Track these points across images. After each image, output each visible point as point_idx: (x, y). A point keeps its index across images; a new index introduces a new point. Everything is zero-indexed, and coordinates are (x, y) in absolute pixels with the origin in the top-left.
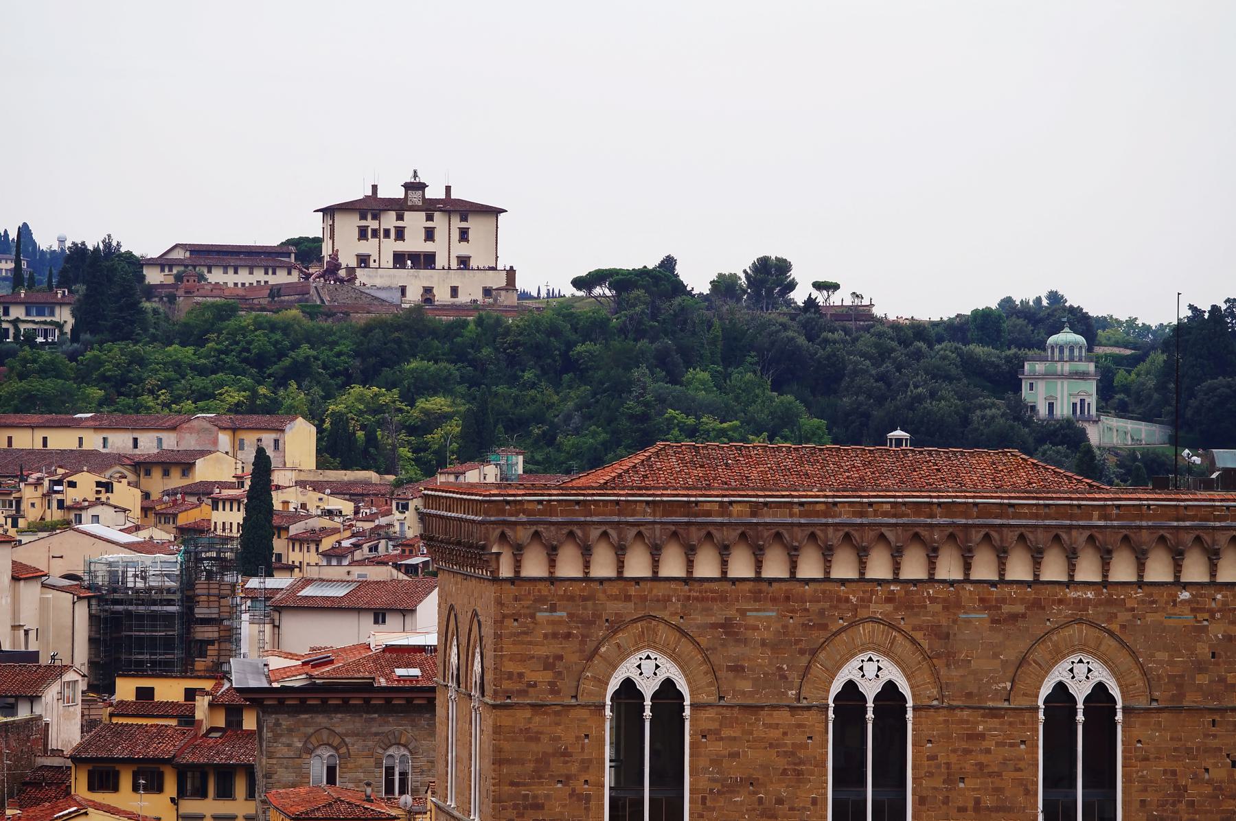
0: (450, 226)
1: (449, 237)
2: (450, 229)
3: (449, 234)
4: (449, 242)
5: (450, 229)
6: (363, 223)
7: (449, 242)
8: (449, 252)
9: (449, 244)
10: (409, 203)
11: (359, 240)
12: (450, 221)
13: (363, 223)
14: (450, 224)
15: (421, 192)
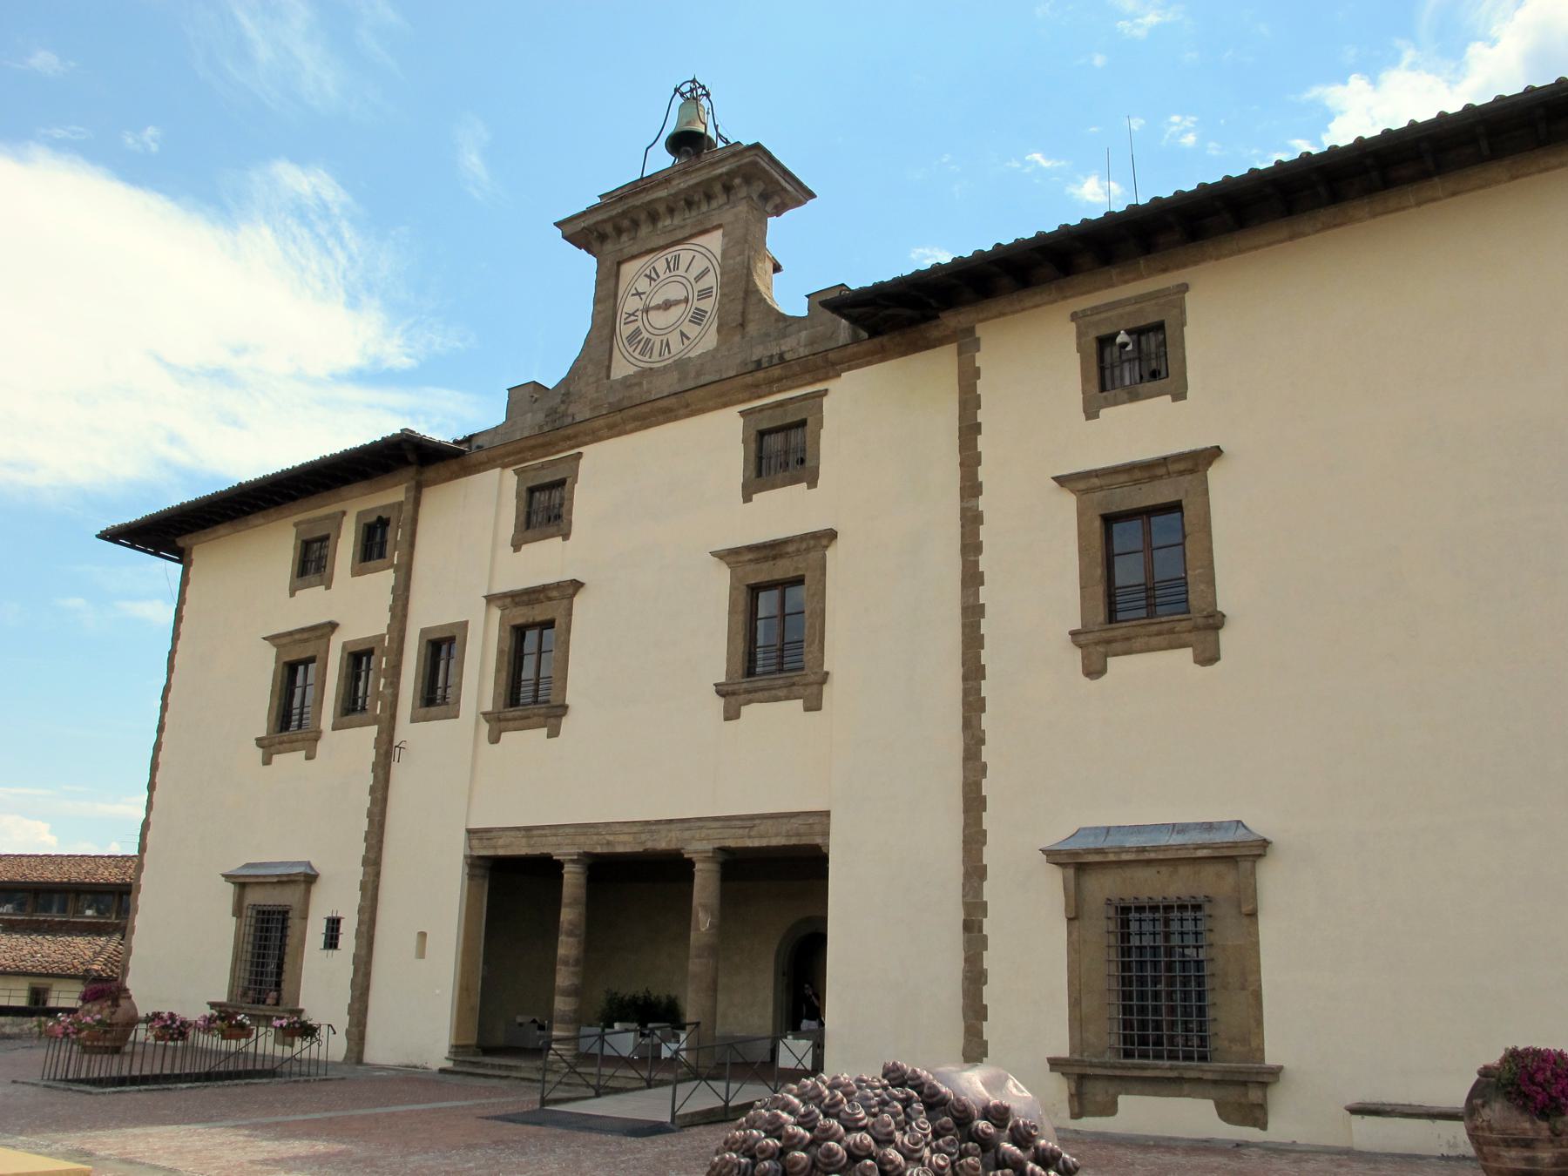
0: (971, 488)
1: (972, 613)
2: (971, 520)
3: (972, 578)
4: (973, 672)
5: (971, 520)
6: (311, 606)
7: (973, 672)
8: (974, 803)
9: (973, 705)
10: (622, 368)
11: (269, 748)
12: (969, 431)
13: (311, 606)
14: (970, 460)
15: (714, 242)
